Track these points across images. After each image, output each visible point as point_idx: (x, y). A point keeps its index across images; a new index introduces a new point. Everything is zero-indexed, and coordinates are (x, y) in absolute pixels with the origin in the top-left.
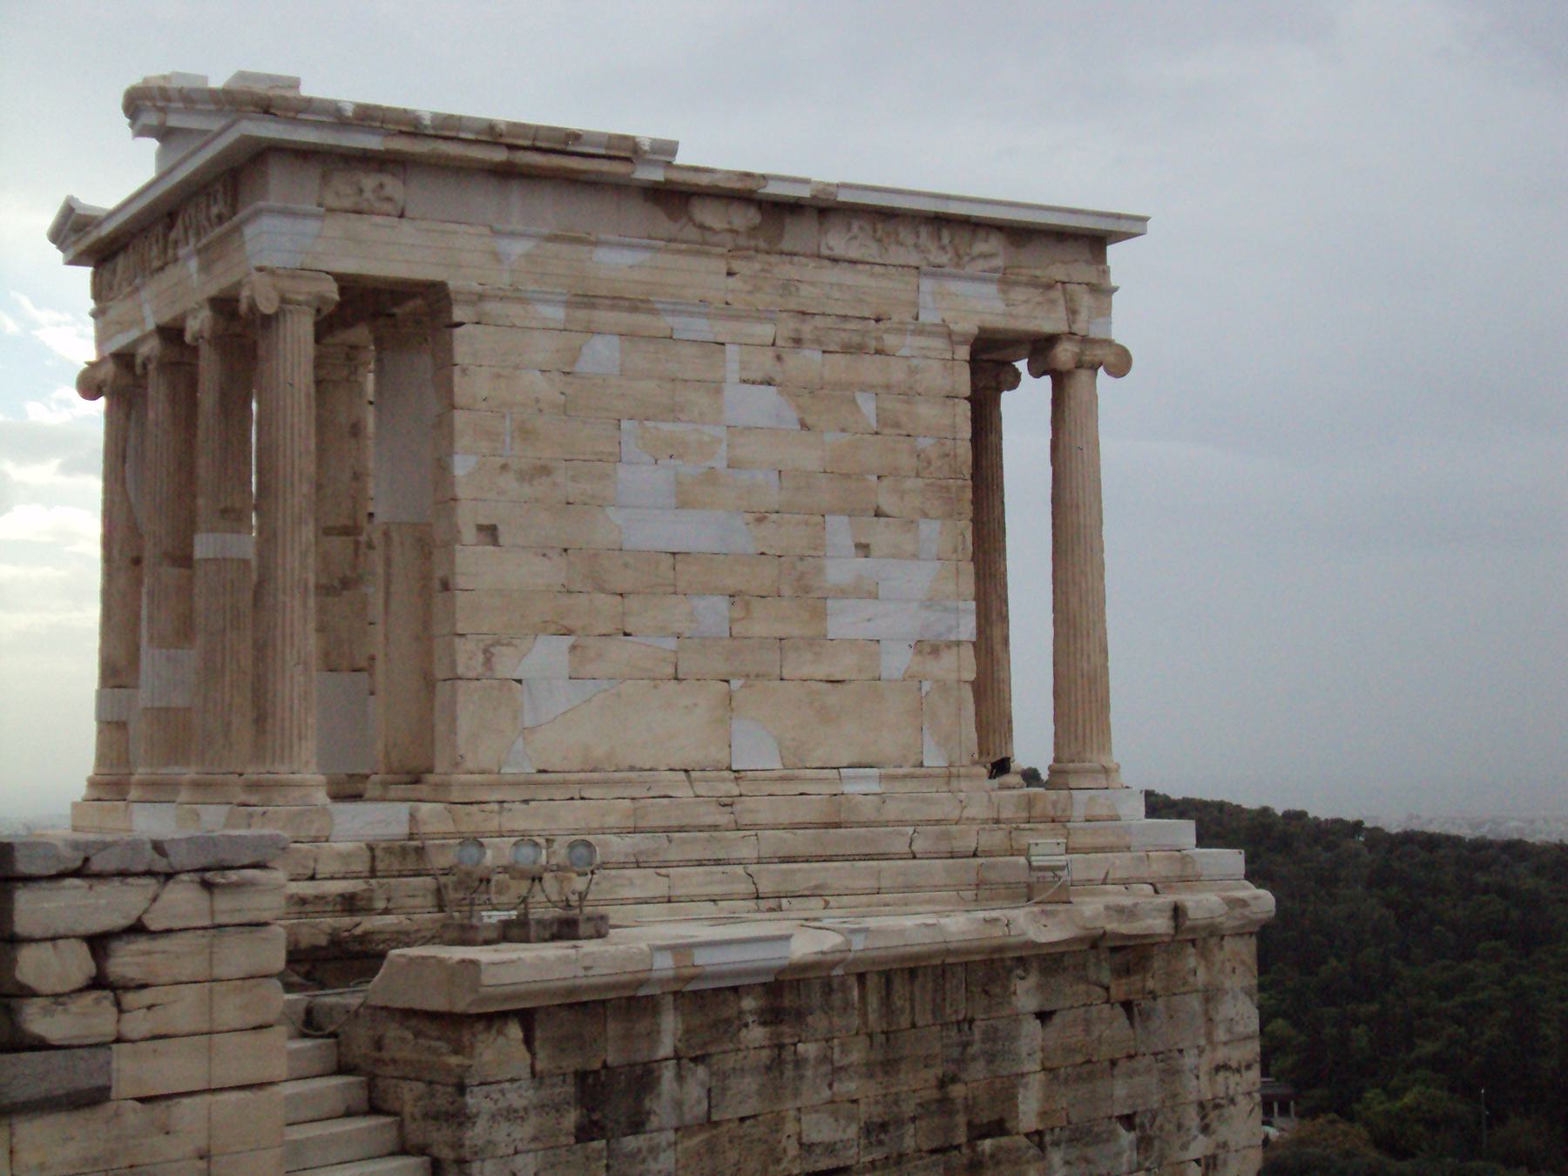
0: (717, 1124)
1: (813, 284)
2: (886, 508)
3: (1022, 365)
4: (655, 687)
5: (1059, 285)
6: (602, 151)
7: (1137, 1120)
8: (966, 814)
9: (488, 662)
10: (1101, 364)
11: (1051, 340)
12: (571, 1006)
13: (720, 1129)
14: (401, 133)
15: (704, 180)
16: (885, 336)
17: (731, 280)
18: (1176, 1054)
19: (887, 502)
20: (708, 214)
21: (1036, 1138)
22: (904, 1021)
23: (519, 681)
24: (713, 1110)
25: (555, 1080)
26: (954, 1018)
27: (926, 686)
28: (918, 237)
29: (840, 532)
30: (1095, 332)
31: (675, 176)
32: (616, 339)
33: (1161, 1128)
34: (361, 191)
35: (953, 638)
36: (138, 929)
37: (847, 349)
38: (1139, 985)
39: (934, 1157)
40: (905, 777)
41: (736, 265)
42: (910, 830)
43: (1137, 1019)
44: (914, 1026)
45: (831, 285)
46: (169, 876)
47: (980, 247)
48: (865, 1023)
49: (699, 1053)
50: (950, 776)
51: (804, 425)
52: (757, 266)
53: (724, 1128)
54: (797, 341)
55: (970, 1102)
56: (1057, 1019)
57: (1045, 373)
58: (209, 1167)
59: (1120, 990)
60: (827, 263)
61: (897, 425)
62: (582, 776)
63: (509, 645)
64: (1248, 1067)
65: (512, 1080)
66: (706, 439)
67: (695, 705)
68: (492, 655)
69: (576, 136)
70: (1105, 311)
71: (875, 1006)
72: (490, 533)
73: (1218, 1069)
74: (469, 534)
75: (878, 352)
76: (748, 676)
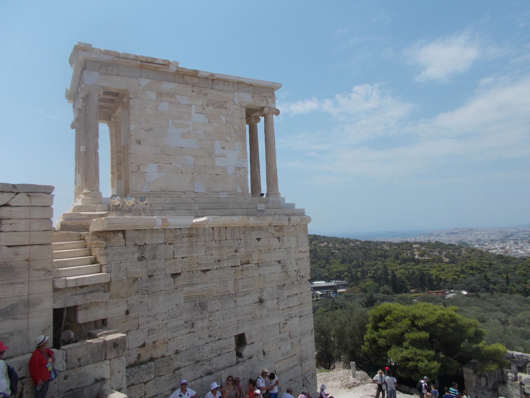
0: (176, 258)
1: (211, 94)
2: (228, 140)
3: (260, 117)
4: (177, 174)
5: (264, 97)
6: (161, 63)
7: (281, 262)
8: (246, 202)
9: (139, 169)
10: (274, 113)
11: (263, 108)
12: (137, 230)
13: (177, 260)
14: (116, 57)
15: (185, 71)
16: (227, 105)
17: (193, 93)
18: (290, 249)
19: (228, 138)
20: (188, 79)
21: (257, 265)
22: (224, 238)
23: (146, 173)
24: (175, 255)
25: (132, 247)
26: (236, 238)
27: (238, 176)
28: (234, 86)
29: (218, 145)
30: (272, 106)
31: (179, 69)
32: (167, 103)
33: (287, 264)
34: (108, 70)
35: (243, 166)
36: (6, 205)
37: (219, 107)
38: (281, 234)
39: (232, 268)
40: (233, 194)
41: (194, 89)
42: (233, 204)
43: (281, 241)
44: (226, 239)
45: (215, 95)
46: (17, 193)
47: (247, 89)
48: (214, 239)
49: (171, 242)
50: (243, 194)
51: (209, 122)
52: (198, 90)
53: (178, 259)
54: (208, 105)
55: (241, 256)
56: (261, 240)
57: (263, 116)
58: (29, 264)
59: (277, 235)
60: (214, 90)
61: (230, 123)
62: (160, 193)
63: (144, 165)
64: (307, 252)
65: (120, 246)
66: (188, 124)
67: (186, 179)
68: (140, 167)
69: (156, 59)
70: (274, 102)
71: (217, 234)
72: (139, 142)
73: (300, 252)
74: (134, 142)
75: (225, 108)
76: (198, 173)
